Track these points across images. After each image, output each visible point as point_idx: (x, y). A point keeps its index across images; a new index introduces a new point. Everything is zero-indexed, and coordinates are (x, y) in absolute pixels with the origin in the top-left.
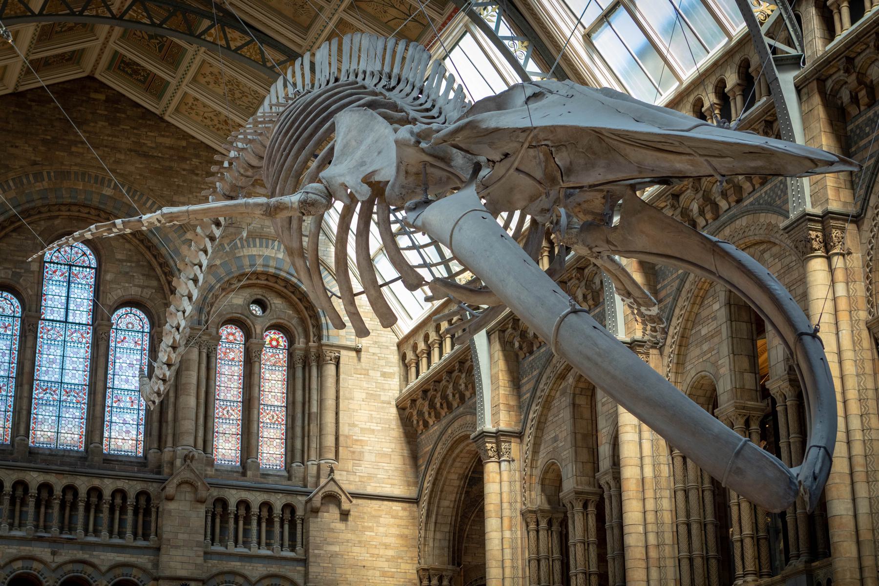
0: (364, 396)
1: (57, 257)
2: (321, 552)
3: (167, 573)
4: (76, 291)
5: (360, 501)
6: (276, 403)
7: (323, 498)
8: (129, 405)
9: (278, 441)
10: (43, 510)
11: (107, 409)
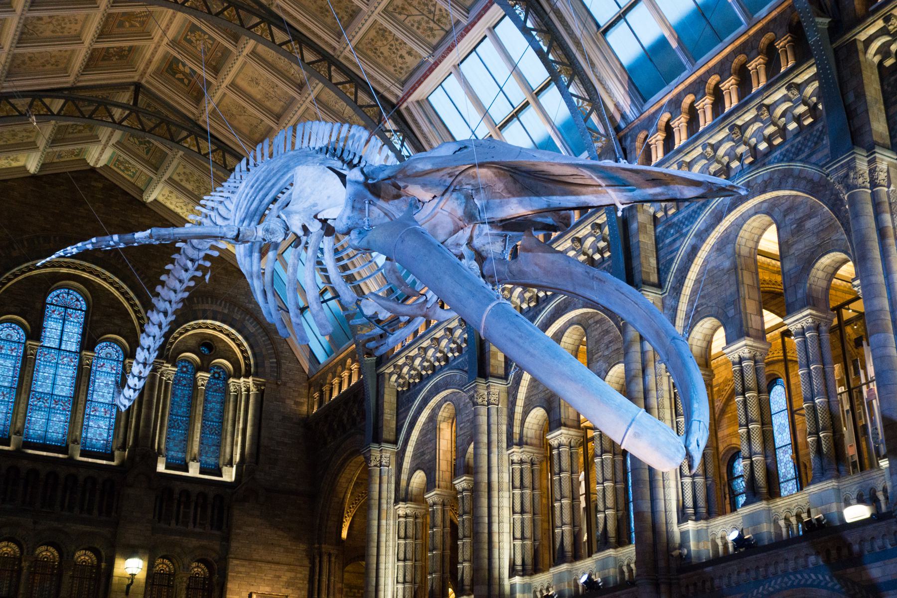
1: (56, 301)
2: (241, 531)
4: (69, 327)
6: (215, 420)
8: (103, 414)
9: (214, 447)
11: (86, 416)
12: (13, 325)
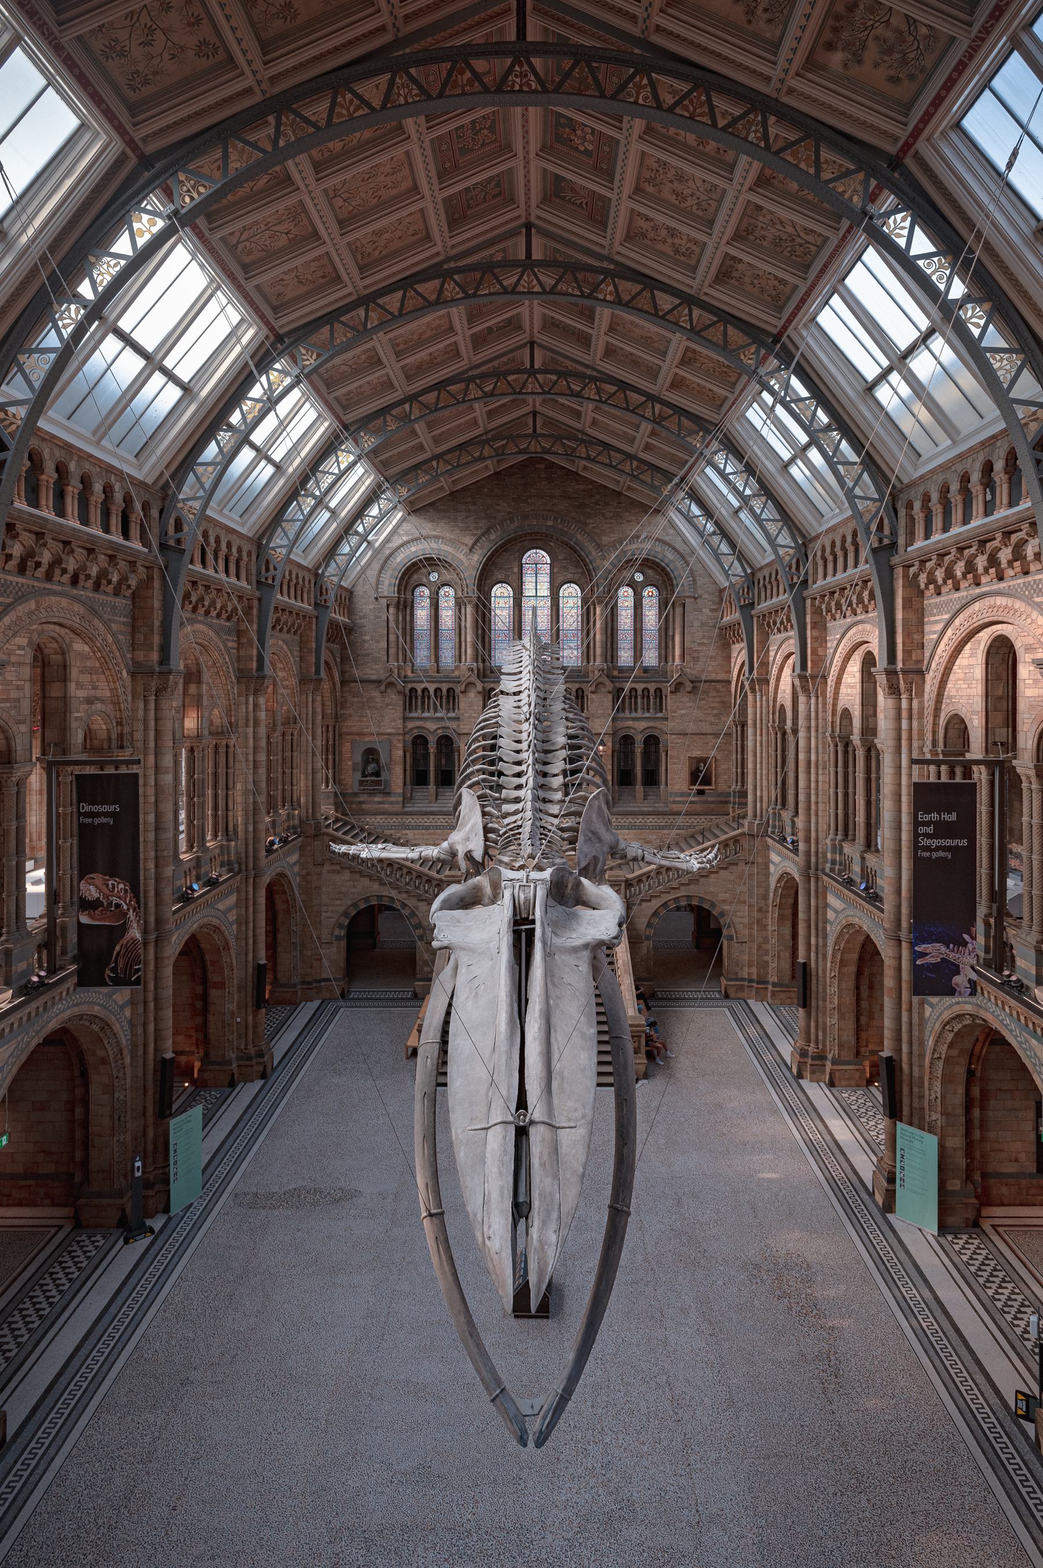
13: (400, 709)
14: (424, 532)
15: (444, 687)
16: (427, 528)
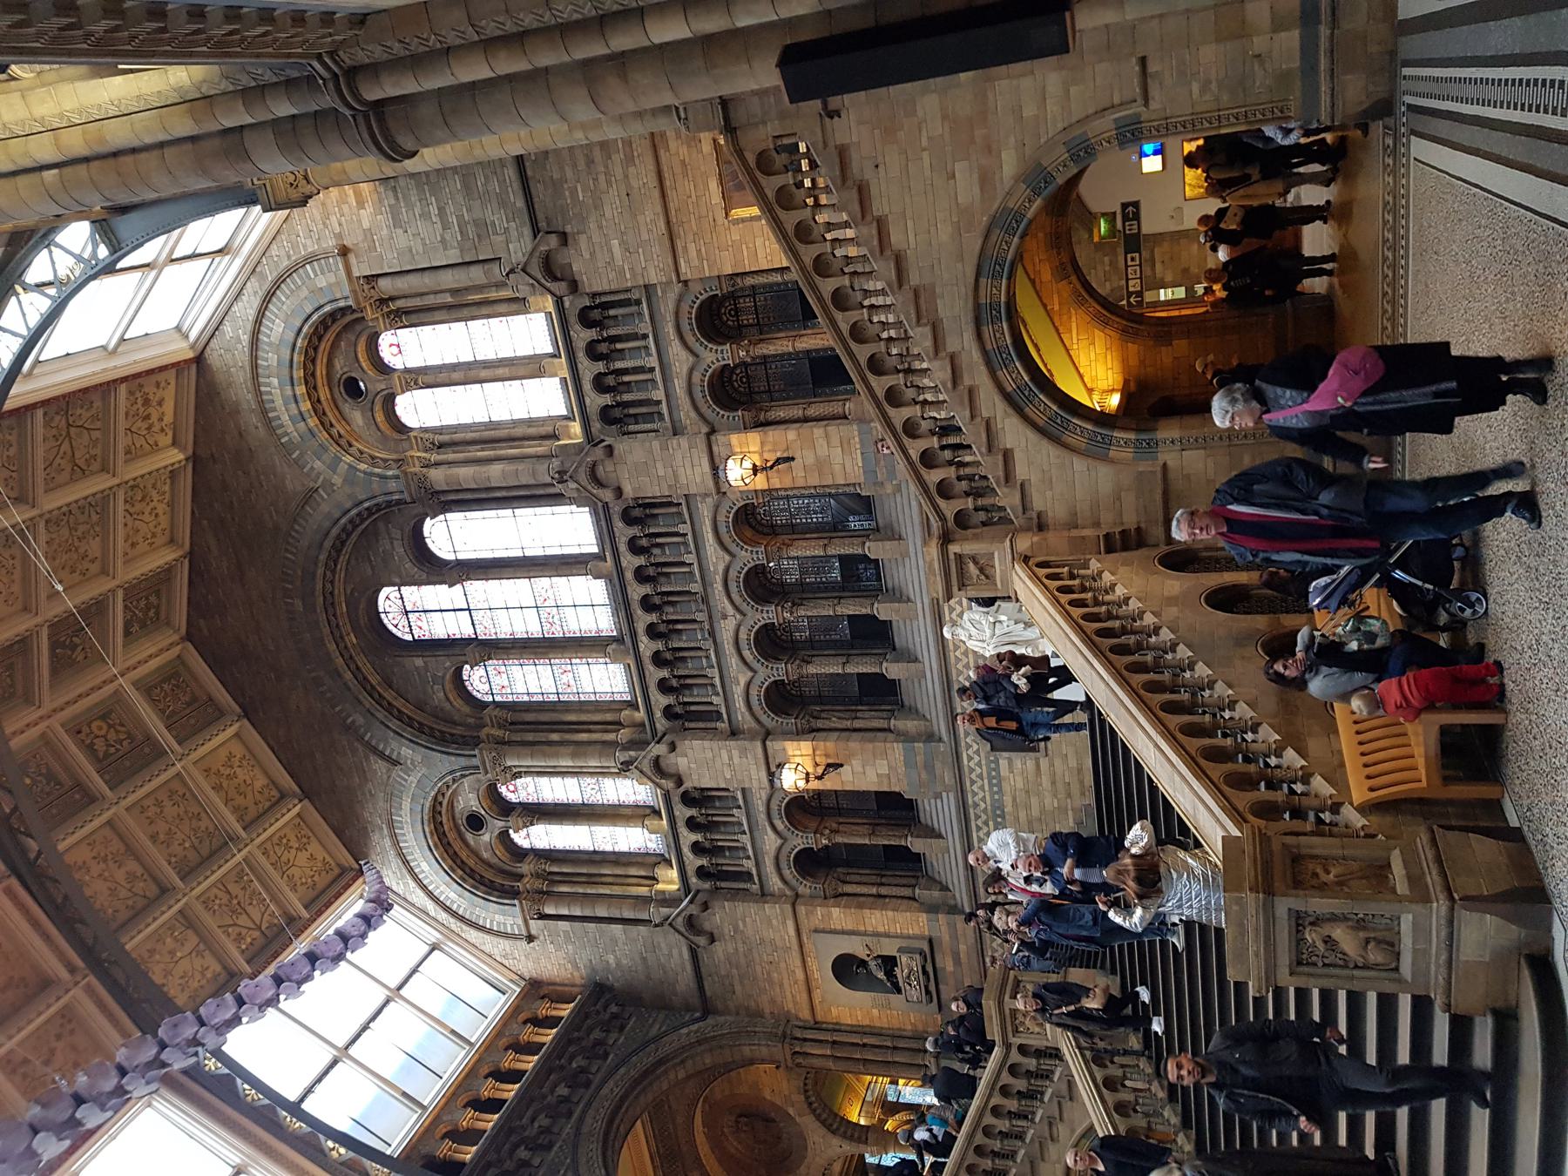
0: (400, 231)
3: (711, 484)
5: (540, 216)
7: (555, 279)
10: (679, 627)
12: (465, 678)
13: (741, 908)
14: (387, 842)
15: (683, 813)
16: (381, 843)
